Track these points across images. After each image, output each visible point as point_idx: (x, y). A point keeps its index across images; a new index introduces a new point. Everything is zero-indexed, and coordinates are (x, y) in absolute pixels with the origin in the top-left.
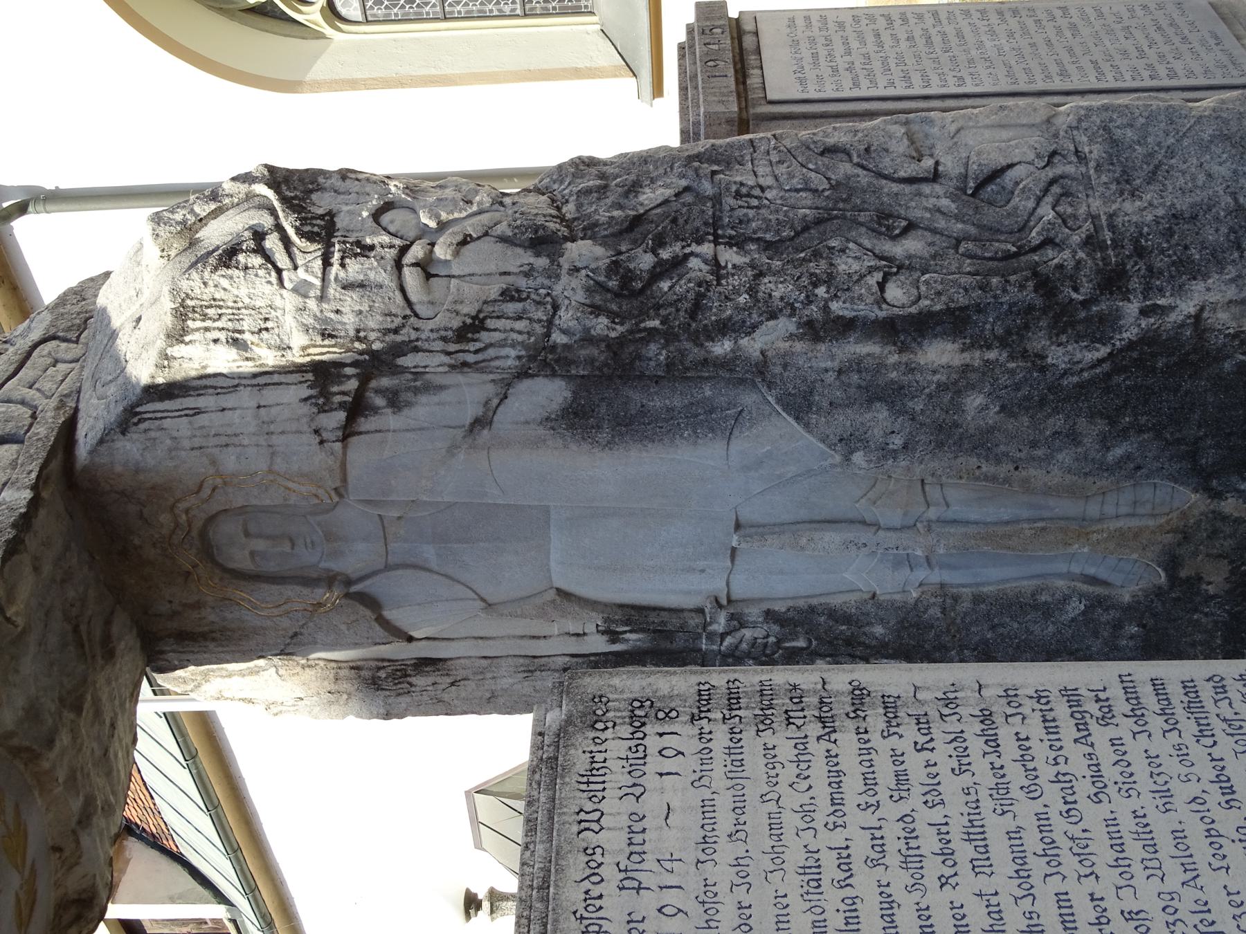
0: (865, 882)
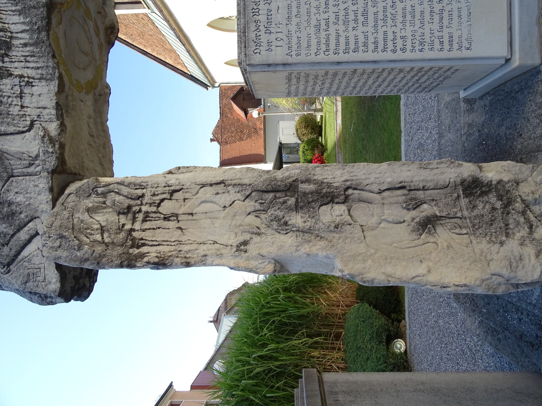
0: (332, 29)
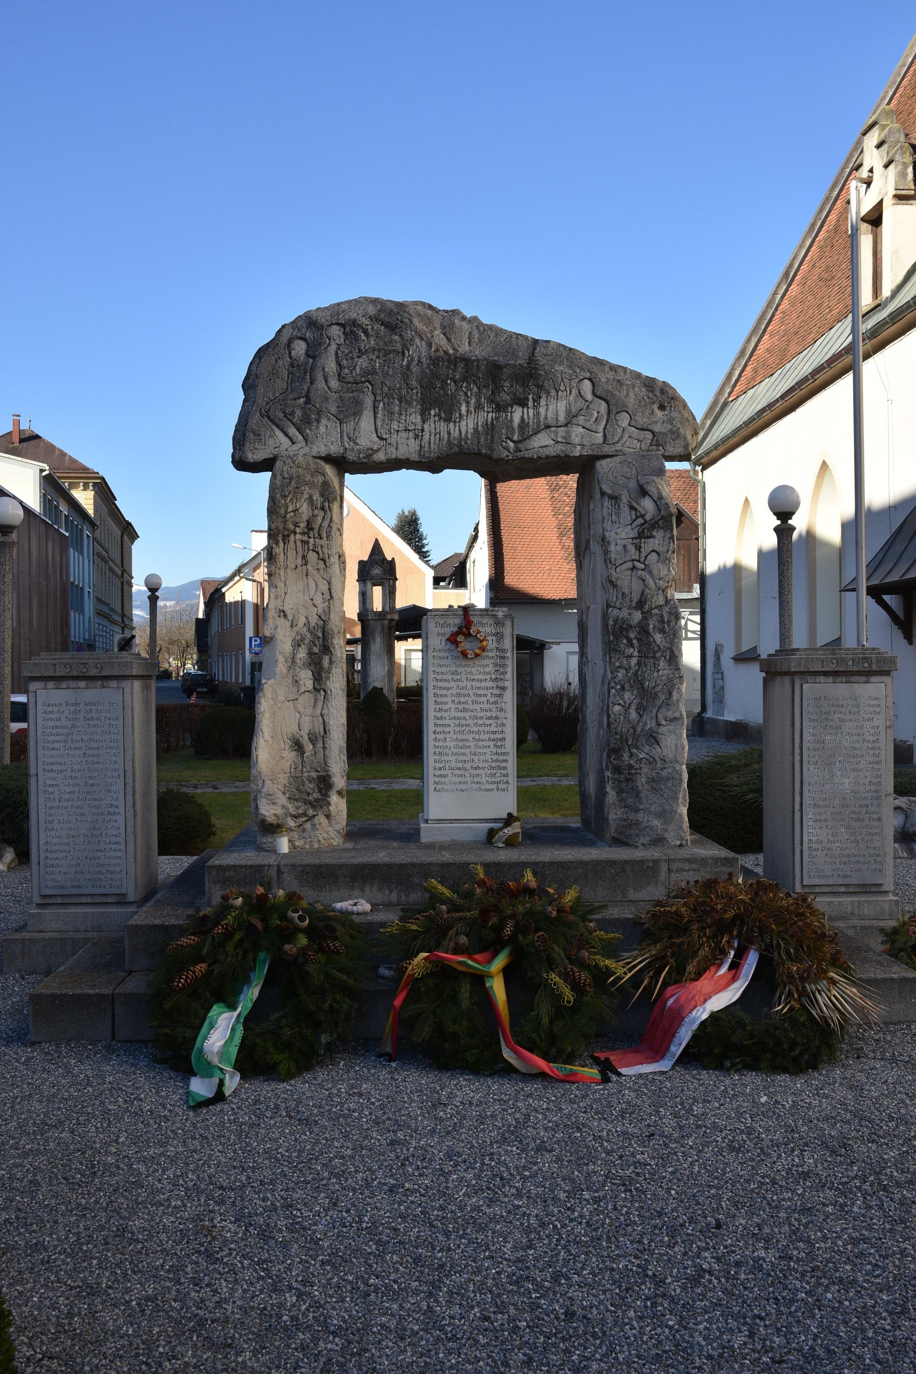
0: (453, 684)
